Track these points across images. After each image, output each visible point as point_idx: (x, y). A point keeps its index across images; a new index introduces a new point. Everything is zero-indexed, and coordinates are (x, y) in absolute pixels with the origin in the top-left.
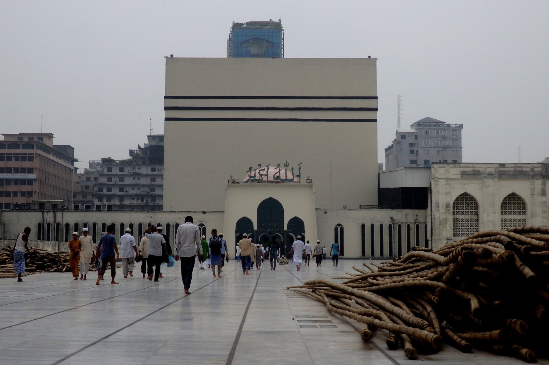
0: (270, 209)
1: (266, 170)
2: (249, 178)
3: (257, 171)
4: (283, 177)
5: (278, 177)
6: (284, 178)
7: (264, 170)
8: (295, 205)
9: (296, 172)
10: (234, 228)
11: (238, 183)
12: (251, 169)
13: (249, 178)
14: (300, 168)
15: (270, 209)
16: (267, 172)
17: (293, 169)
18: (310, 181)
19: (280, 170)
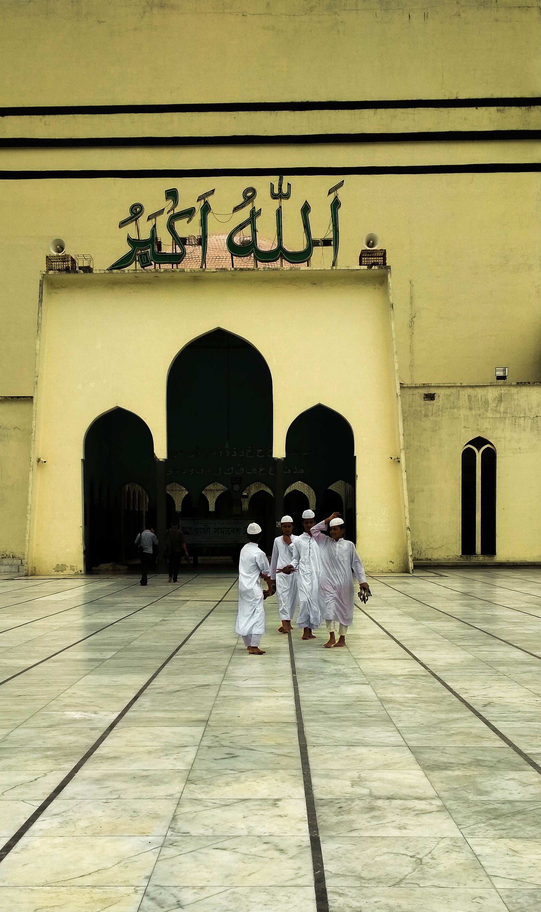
0: (219, 376)
1: (197, 217)
2: (128, 249)
3: (162, 221)
4: (267, 243)
5: (243, 243)
6: (275, 247)
7: (189, 213)
8: (317, 358)
9: (321, 229)
10: (76, 453)
11: (88, 270)
12: (136, 211)
13: (128, 249)
14: (336, 205)
15: (219, 376)
16: (204, 223)
17: (306, 209)
18: (380, 260)
19: (254, 214)
